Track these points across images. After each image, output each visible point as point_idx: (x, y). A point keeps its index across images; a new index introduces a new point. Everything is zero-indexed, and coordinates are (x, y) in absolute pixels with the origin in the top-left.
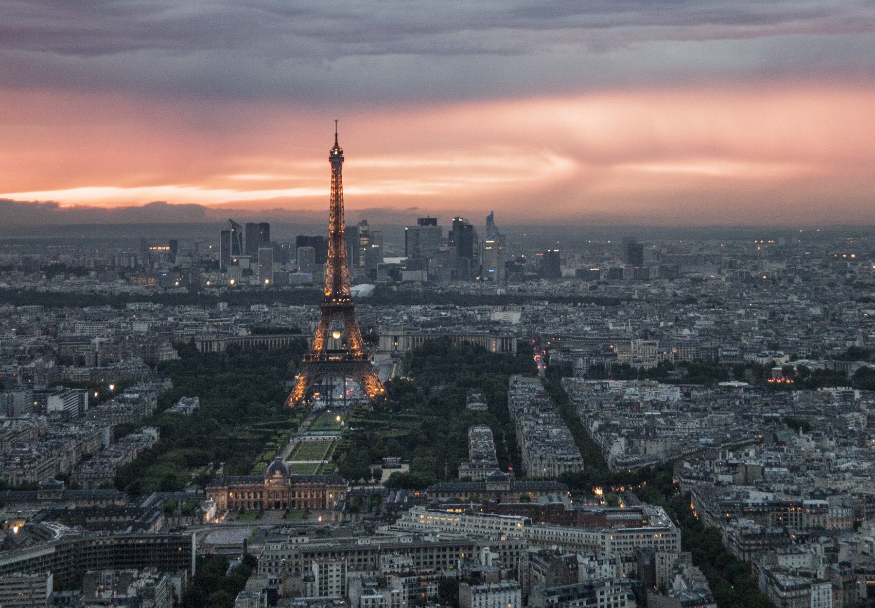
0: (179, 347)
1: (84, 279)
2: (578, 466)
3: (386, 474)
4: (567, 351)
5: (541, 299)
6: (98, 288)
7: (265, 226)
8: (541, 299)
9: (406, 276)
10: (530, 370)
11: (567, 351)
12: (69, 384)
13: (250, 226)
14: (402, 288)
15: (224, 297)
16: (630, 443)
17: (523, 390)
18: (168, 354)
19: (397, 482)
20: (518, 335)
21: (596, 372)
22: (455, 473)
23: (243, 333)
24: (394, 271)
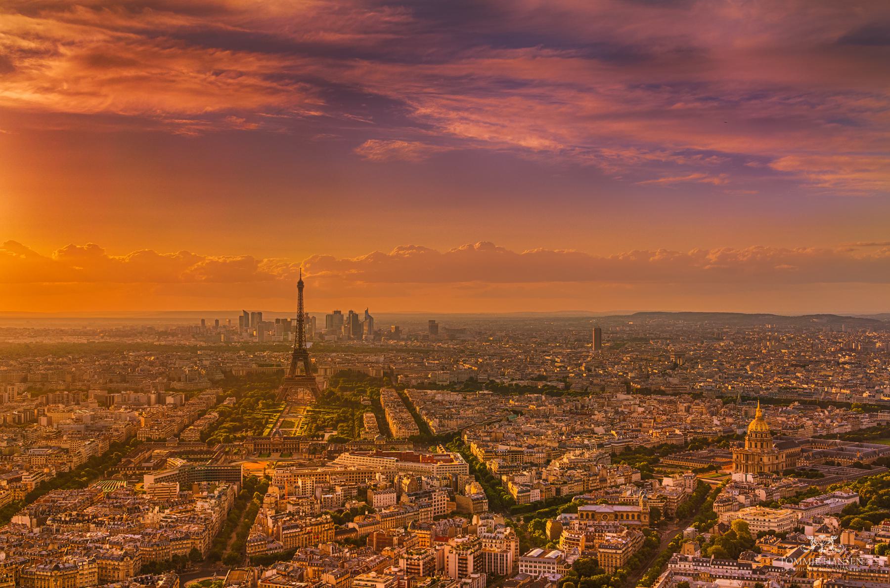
0: (224, 372)
1: (175, 338)
2: (416, 432)
3: (327, 436)
4: (406, 376)
5: (392, 350)
6: (182, 342)
7: (260, 314)
8: (392, 350)
9: (327, 338)
10: (389, 384)
11: (406, 376)
12: (173, 390)
13: (253, 313)
14: (326, 344)
15: (243, 348)
16: (440, 422)
17: (386, 396)
18: (219, 376)
19: (333, 440)
20: (383, 368)
21: (421, 386)
22: (359, 435)
23: (254, 366)
24: (321, 336)
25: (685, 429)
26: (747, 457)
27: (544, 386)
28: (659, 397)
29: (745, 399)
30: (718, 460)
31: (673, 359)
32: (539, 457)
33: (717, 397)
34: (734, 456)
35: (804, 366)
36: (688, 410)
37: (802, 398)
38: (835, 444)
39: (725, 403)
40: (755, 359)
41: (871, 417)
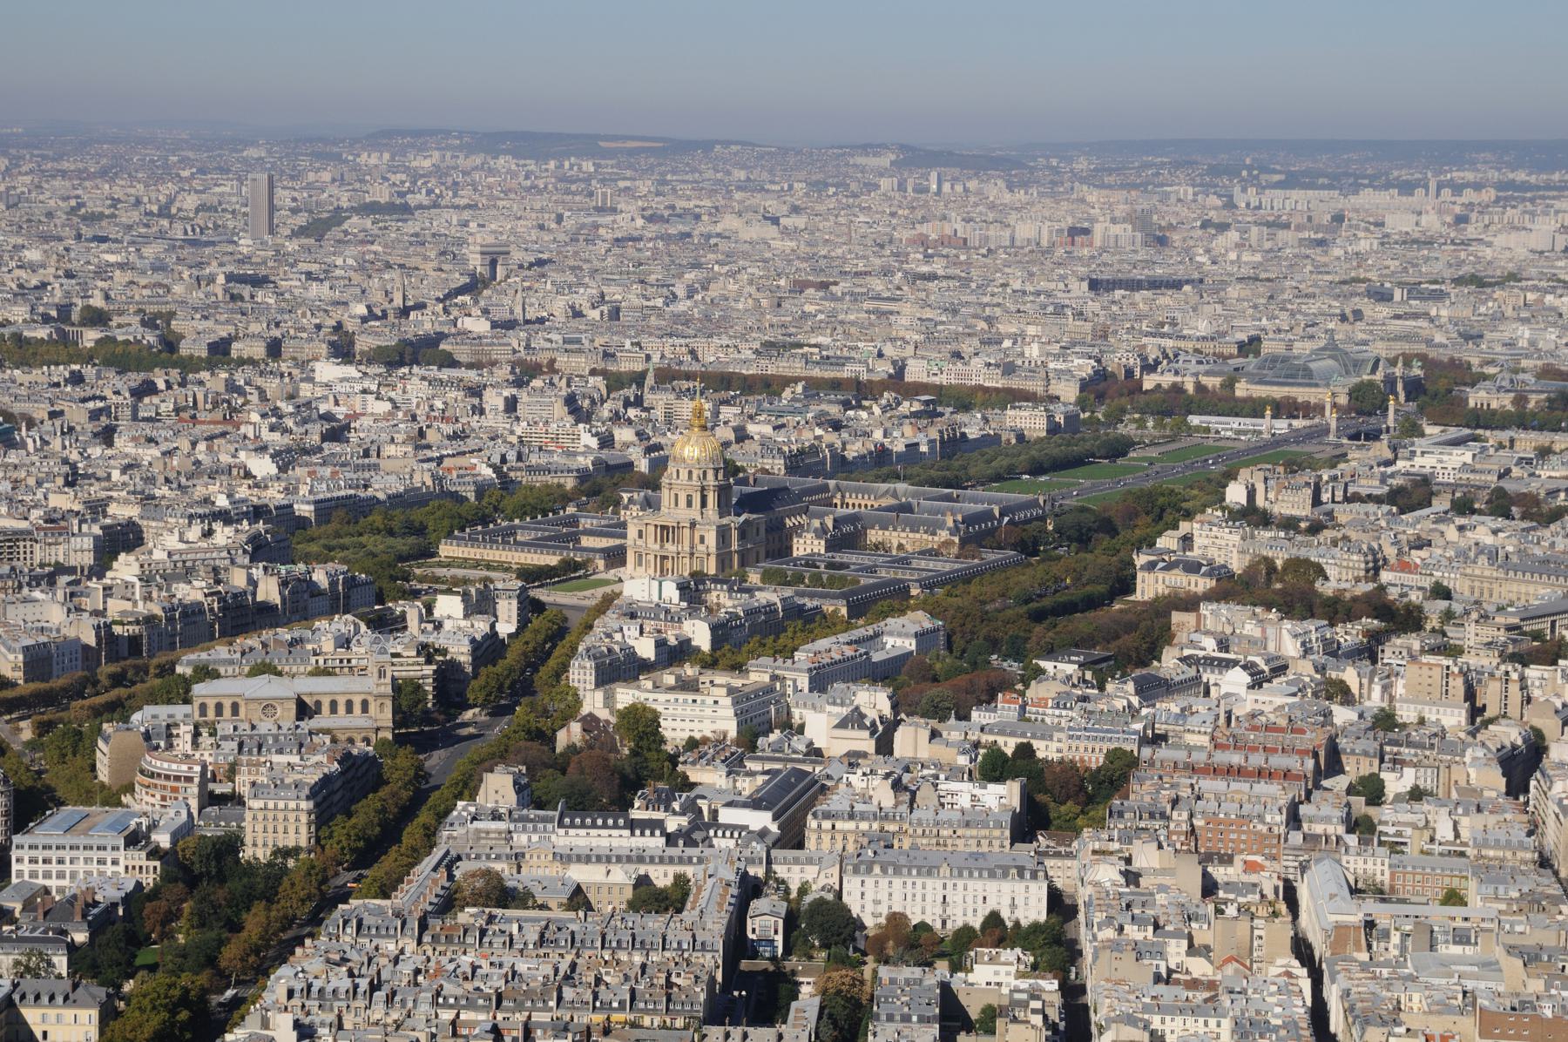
25: (504, 460)
26: (666, 532)
27: (98, 342)
28: (433, 371)
29: (666, 377)
30: (586, 542)
31: (476, 262)
32: (79, 550)
33: (593, 372)
34: (632, 532)
35: (824, 286)
36: (511, 405)
37: (816, 372)
38: (895, 495)
39: (610, 389)
40: (696, 266)
41: (986, 420)
